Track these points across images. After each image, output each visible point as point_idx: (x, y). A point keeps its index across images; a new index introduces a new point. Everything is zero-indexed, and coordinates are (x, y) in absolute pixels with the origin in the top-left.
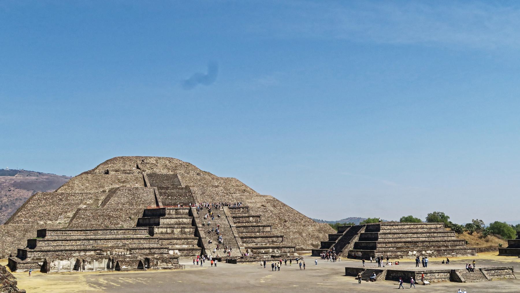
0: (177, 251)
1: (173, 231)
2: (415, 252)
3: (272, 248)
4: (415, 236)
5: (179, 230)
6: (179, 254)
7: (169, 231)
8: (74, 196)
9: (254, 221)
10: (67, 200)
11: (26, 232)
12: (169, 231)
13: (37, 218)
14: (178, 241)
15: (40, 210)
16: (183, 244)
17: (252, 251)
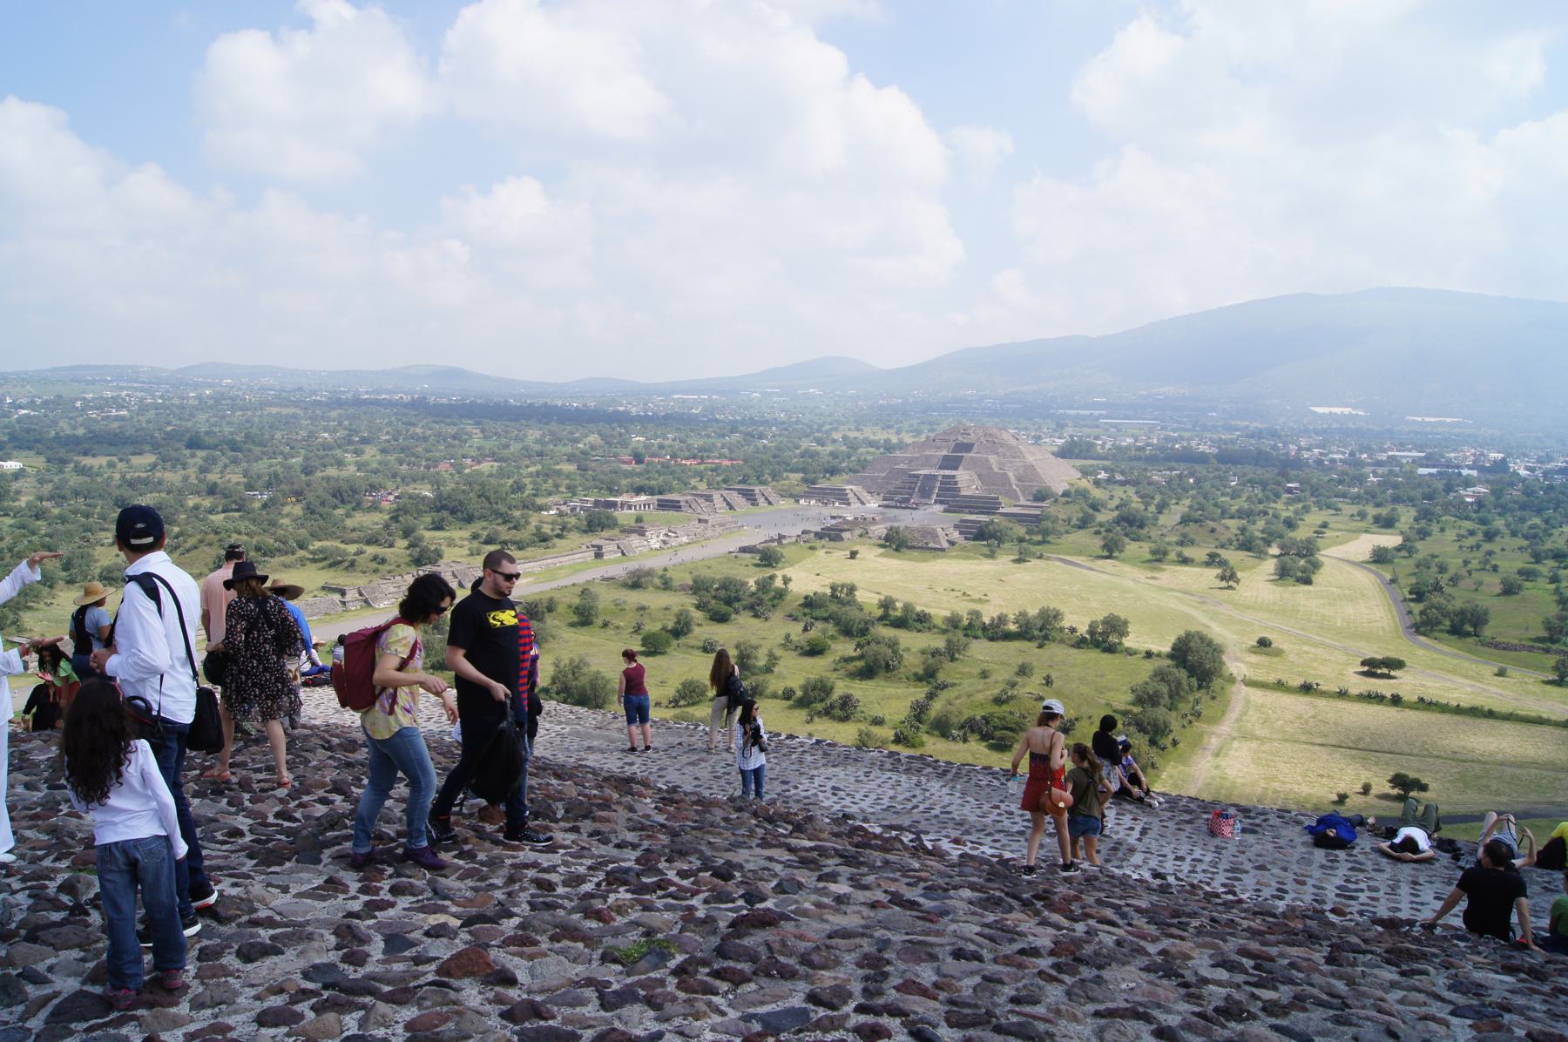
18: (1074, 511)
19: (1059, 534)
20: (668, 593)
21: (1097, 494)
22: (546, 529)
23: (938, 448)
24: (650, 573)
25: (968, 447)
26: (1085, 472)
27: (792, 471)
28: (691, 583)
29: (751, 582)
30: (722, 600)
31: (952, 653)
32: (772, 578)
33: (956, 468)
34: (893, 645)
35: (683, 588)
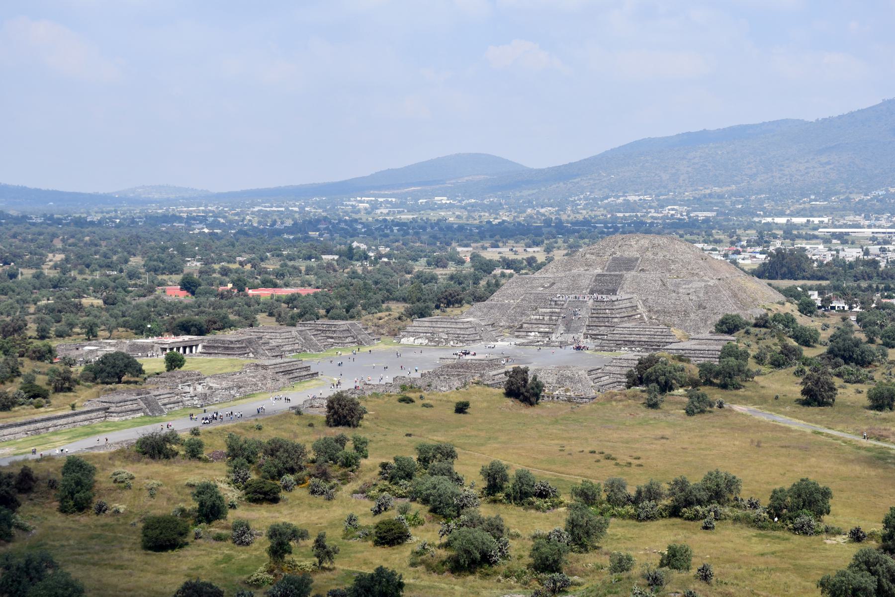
7: (541, 318)
12: (541, 318)
15: (509, 291)
18: (773, 344)
19: (749, 375)
20: (194, 463)
21: (803, 321)
22: (41, 381)
23: (589, 265)
24: (172, 438)
25: (628, 264)
26: (790, 294)
27: (397, 300)
28: (225, 450)
29: (309, 447)
30: (268, 469)
31: (581, 536)
32: (341, 441)
33: (614, 292)
34: (496, 529)
35: (217, 457)
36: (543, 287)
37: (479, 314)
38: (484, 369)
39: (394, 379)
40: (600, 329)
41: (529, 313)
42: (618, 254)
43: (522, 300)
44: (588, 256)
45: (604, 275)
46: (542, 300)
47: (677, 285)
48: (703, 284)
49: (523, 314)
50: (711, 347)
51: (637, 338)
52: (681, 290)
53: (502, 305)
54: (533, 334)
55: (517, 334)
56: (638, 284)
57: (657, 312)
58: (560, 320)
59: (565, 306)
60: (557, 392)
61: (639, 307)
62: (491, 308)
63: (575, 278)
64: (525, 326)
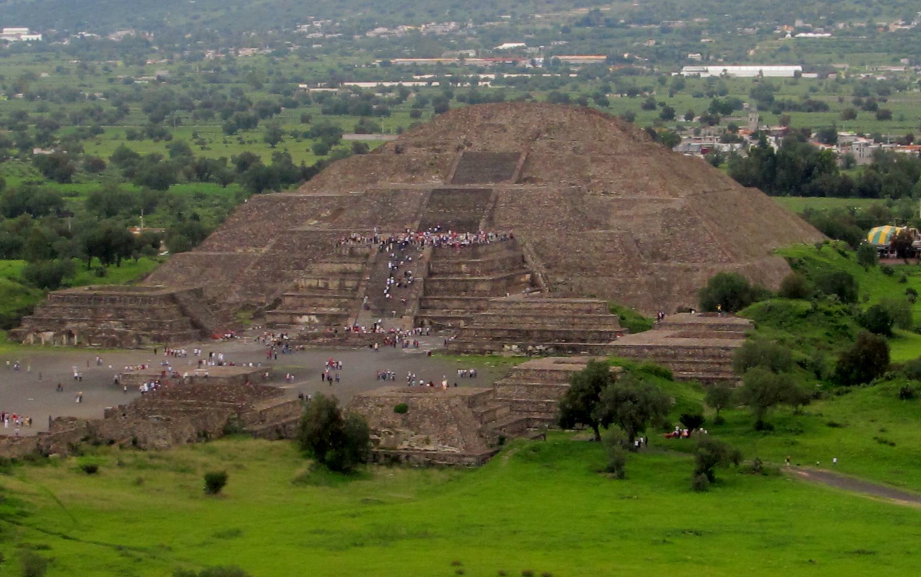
0: (313, 318)
1: (327, 285)
2: (514, 347)
3: (464, 319)
4: (539, 321)
5: (336, 283)
6: (317, 321)
8: (305, 202)
9: (469, 270)
10: (292, 209)
11: (207, 266)
12: (321, 284)
13: (236, 241)
14: (326, 302)
15: (245, 229)
16: (333, 306)
17: (431, 323)
33: (471, 226)
36: (318, 218)
37: (181, 277)
38: (242, 399)
39: (52, 423)
40: (450, 305)
41: (288, 272)
42: (477, 146)
43: (275, 247)
44: (410, 151)
45: (449, 191)
46: (320, 247)
47: (605, 211)
48: (659, 208)
49: (278, 276)
50: (711, 342)
51: (537, 325)
52: (613, 221)
53: (231, 258)
54: (305, 319)
55: (270, 319)
56: (524, 210)
57: (568, 267)
58: (362, 290)
59: (371, 260)
60: (405, 445)
61: (528, 258)
62: (209, 265)
63: (388, 199)
64: (288, 301)
